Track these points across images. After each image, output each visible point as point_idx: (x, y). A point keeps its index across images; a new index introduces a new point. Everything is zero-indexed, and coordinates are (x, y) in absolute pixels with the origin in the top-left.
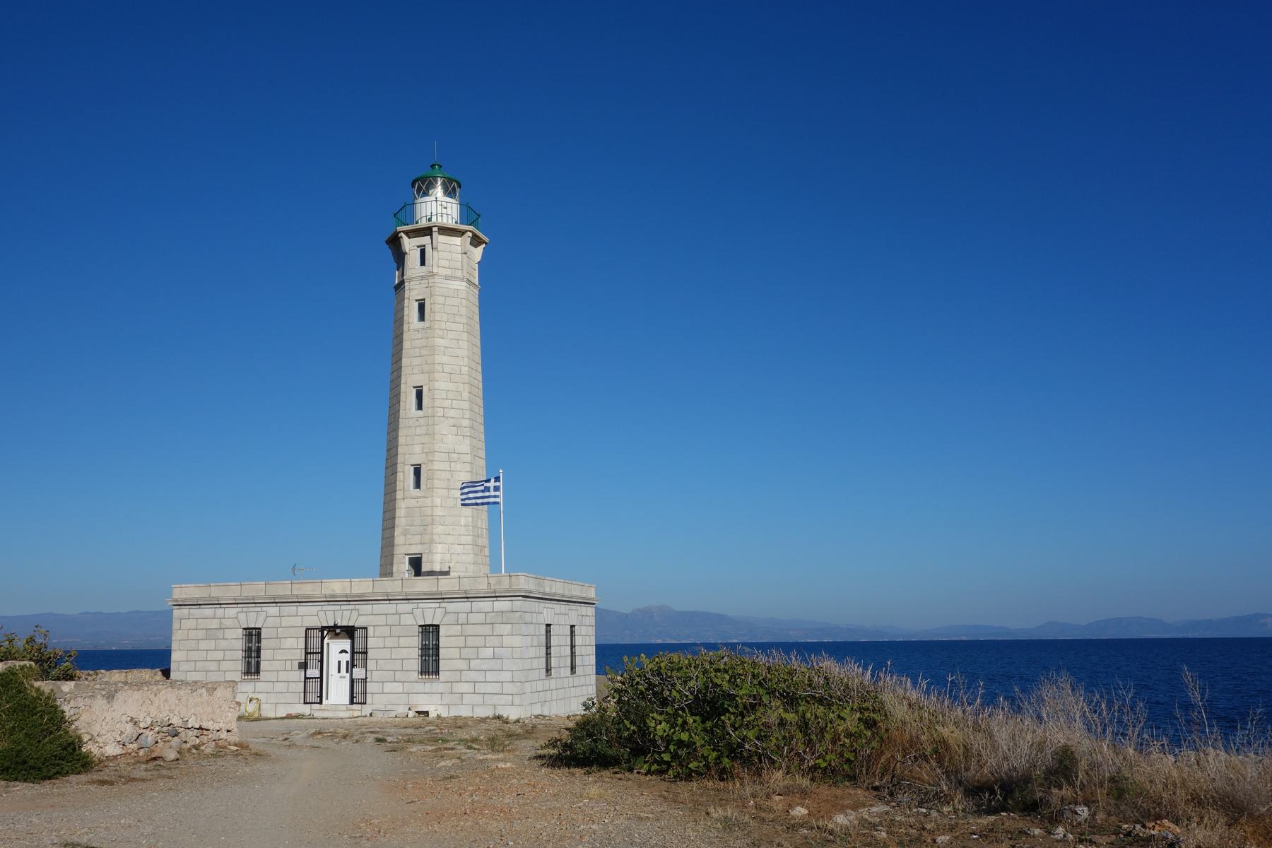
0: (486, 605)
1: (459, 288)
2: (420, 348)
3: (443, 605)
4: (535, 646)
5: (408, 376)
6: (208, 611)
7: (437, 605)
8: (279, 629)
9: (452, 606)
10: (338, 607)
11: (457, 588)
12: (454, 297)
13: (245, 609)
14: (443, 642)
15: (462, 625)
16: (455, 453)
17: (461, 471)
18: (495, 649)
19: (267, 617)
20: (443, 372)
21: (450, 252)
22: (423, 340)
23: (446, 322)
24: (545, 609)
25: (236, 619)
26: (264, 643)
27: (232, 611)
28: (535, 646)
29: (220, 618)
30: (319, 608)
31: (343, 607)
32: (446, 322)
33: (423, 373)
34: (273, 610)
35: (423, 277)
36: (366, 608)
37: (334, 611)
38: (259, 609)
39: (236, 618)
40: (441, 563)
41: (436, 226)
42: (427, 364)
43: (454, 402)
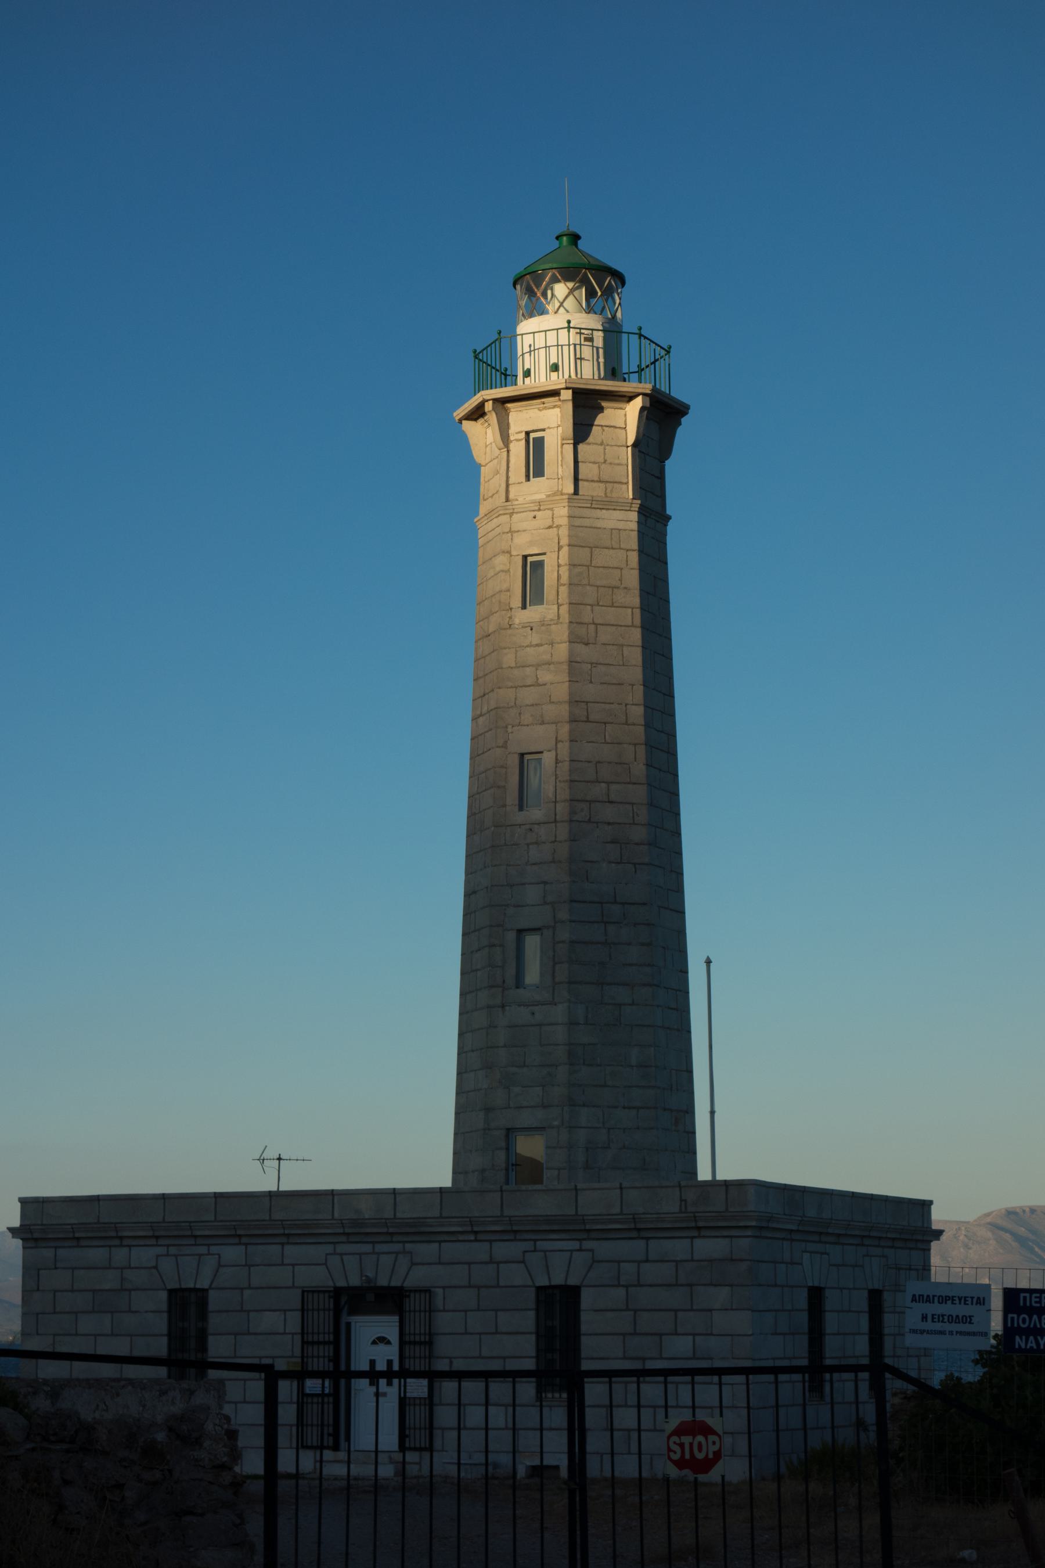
0: (678, 1248)
1: (621, 525)
2: (537, 666)
3: (587, 1245)
4: (784, 1334)
5: (510, 730)
6: (96, 1254)
7: (576, 1245)
8: (247, 1293)
9: (604, 1249)
10: (368, 1248)
11: (617, 1210)
12: (612, 548)
13: (173, 1250)
14: (588, 1321)
15: (627, 1287)
16: (615, 902)
17: (629, 944)
18: (697, 1338)
19: (220, 1265)
20: (588, 721)
21: (602, 444)
22: (541, 649)
23: (592, 606)
24: (806, 1256)
25: (154, 1271)
26: (214, 1321)
27: (144, 1255)
28: (784, 1334)
29: (122, 1268)
30: (330, 1248)
31: (379, 1248)
32: (592, 606)
33: (543, 723)
34: (232, 1253)
35: (540, 503)
36: (427, 1250)
37: (360, 1254)
38: (203, 1250)
39: (156, 1267)
40: (587, 1149)
41: (567, 388)
42: (551, 702)
43: (613, 787)
